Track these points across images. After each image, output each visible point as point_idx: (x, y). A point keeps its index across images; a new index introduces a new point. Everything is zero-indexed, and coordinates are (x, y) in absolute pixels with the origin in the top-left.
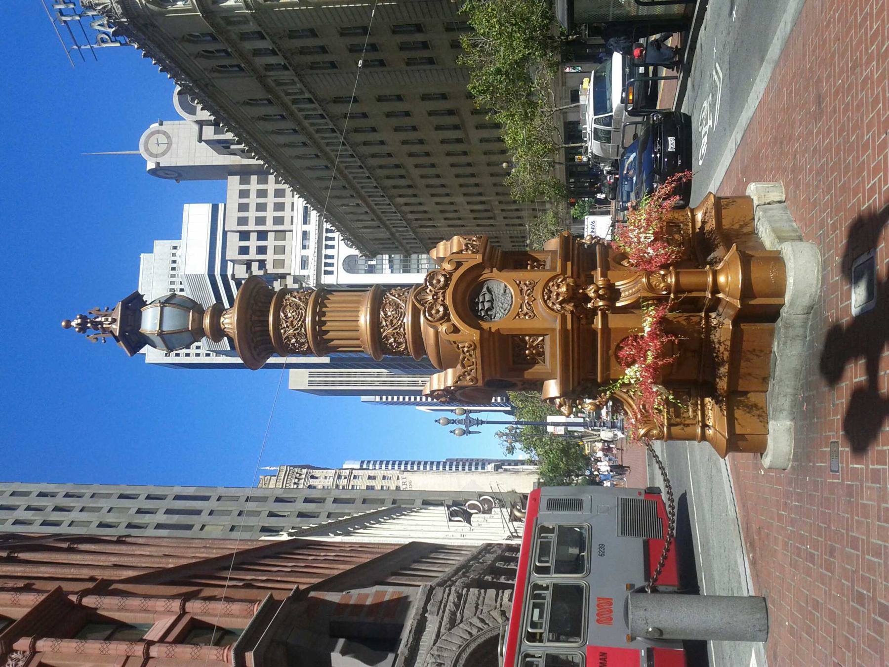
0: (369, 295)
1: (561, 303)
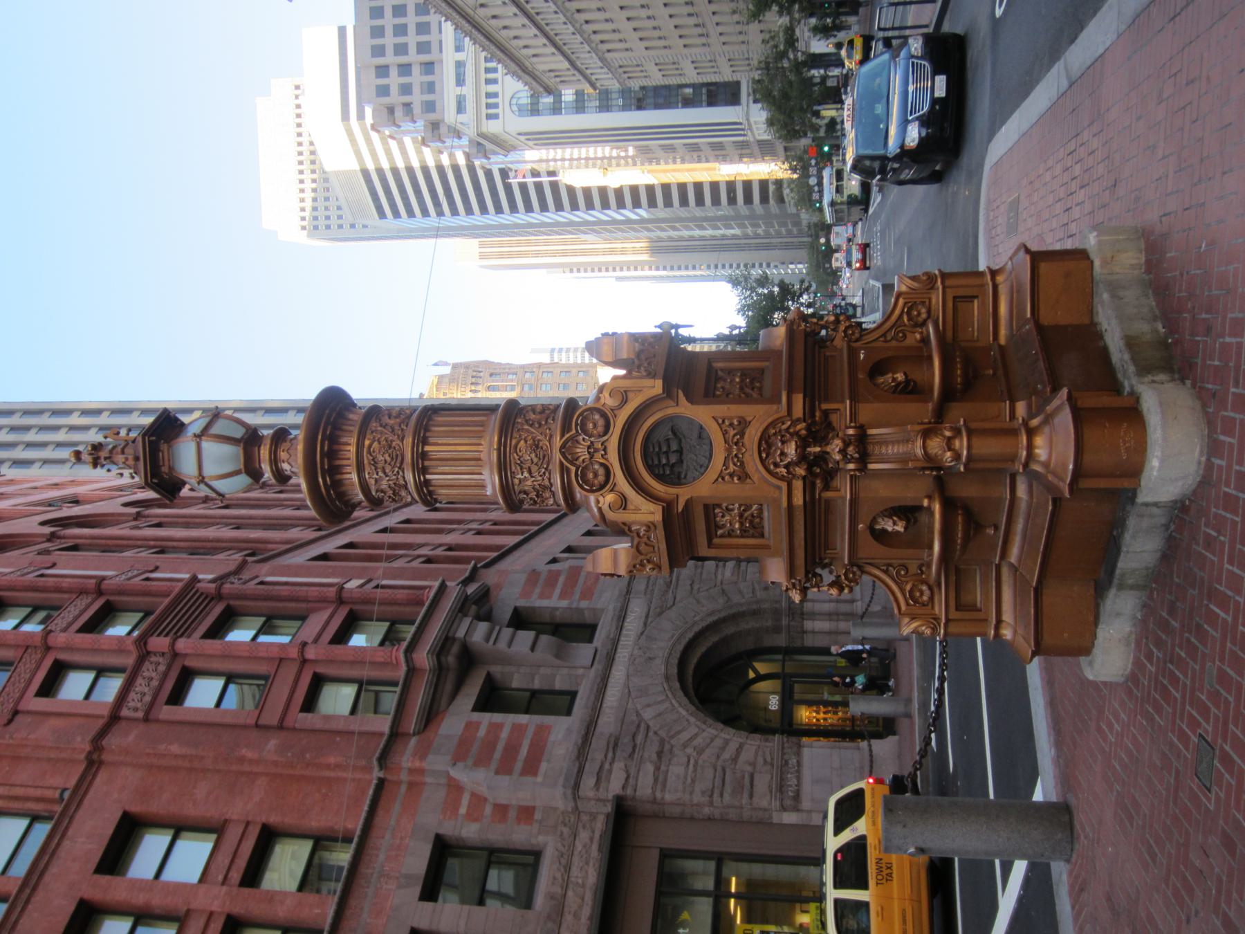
0: (495, 421)
1: (786, 467)
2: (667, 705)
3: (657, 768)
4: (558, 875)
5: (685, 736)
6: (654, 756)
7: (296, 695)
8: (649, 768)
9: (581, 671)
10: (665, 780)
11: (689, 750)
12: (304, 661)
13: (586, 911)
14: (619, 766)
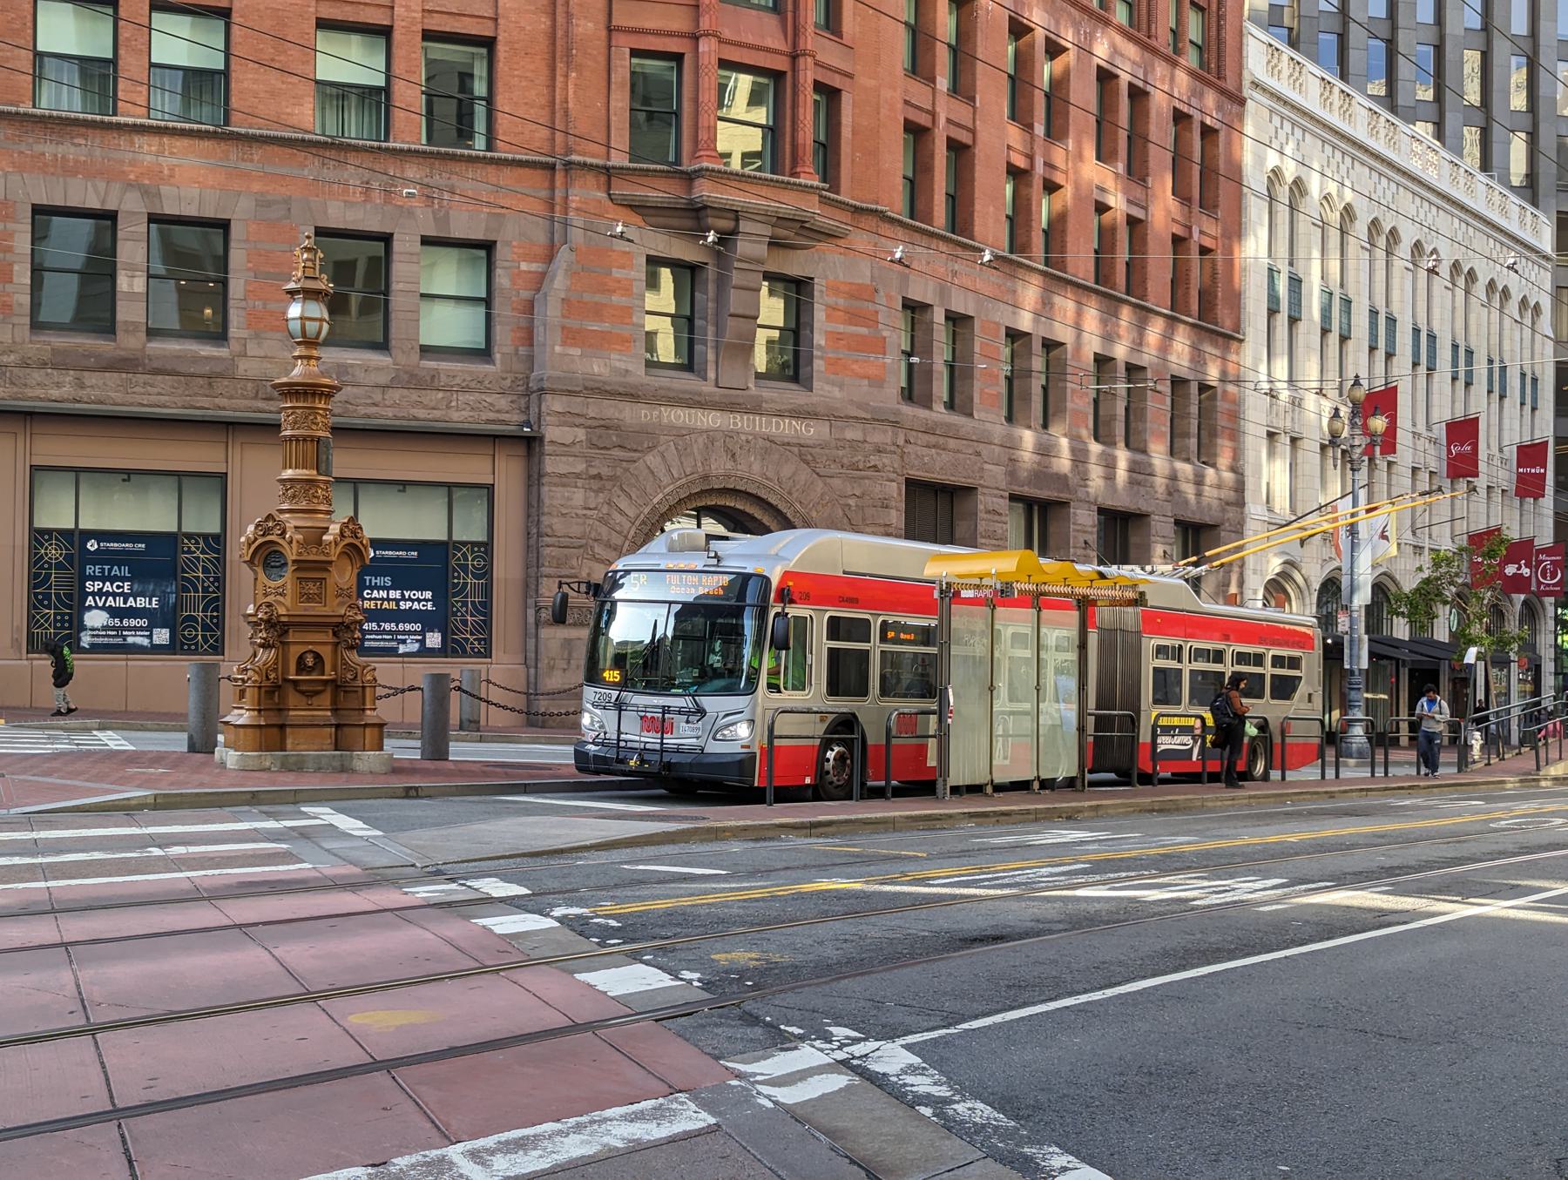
2: (666, 480)
3: (578, 476)
4: (458, 381)
5: (623, 504)
6: (593, 471)
7: (651, 39)
8: (580, 467)
9: (711, 375)
10: (564, 485)
11: (605, 509)
12: (695, 38)
13: (421, 413)
14: (581, 434)
